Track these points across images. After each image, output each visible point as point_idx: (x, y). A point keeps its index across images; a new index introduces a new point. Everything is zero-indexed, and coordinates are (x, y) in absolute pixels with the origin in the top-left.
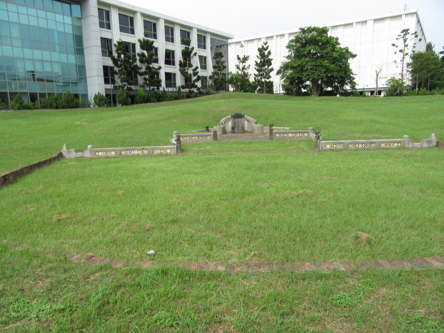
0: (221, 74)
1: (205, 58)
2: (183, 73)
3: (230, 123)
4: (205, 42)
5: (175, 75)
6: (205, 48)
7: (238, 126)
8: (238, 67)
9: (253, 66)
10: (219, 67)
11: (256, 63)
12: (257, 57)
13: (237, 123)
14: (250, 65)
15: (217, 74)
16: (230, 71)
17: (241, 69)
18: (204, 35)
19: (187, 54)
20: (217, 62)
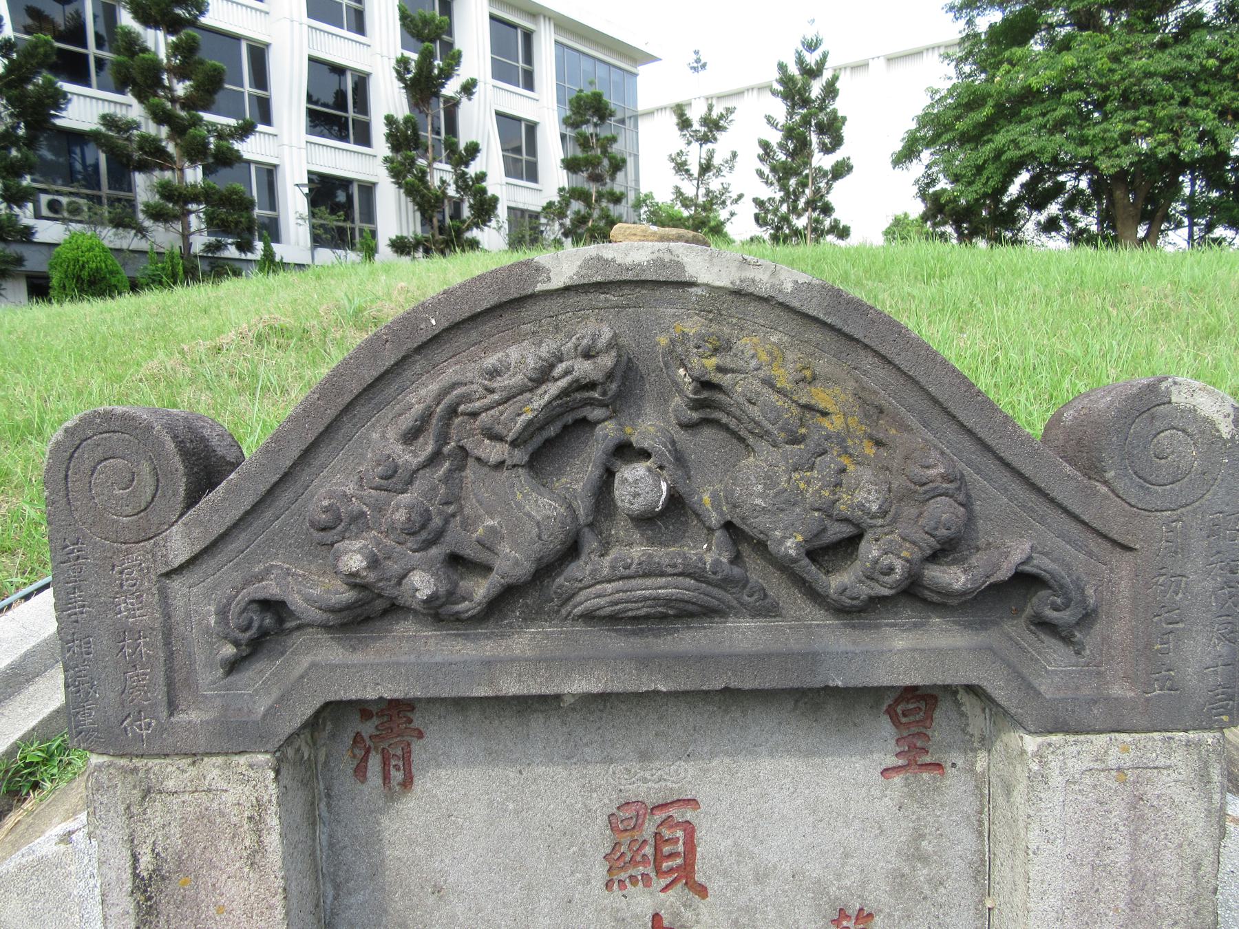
0: (600, 196)
1: (532, 128)
2: (397, 173)
4: (529, 58)
5: (368, 190)
6: (529, 84)
8: (681, 168)
9: (750, 160)
10: (592, 163)
11: (765, 145)
12: (770, 120)
14: (734, 155)
15: (582, 195)
16: (644, 190)
17: (695, 170)
18: (528, 25)
19: (422, 85)
20: (584, 142)
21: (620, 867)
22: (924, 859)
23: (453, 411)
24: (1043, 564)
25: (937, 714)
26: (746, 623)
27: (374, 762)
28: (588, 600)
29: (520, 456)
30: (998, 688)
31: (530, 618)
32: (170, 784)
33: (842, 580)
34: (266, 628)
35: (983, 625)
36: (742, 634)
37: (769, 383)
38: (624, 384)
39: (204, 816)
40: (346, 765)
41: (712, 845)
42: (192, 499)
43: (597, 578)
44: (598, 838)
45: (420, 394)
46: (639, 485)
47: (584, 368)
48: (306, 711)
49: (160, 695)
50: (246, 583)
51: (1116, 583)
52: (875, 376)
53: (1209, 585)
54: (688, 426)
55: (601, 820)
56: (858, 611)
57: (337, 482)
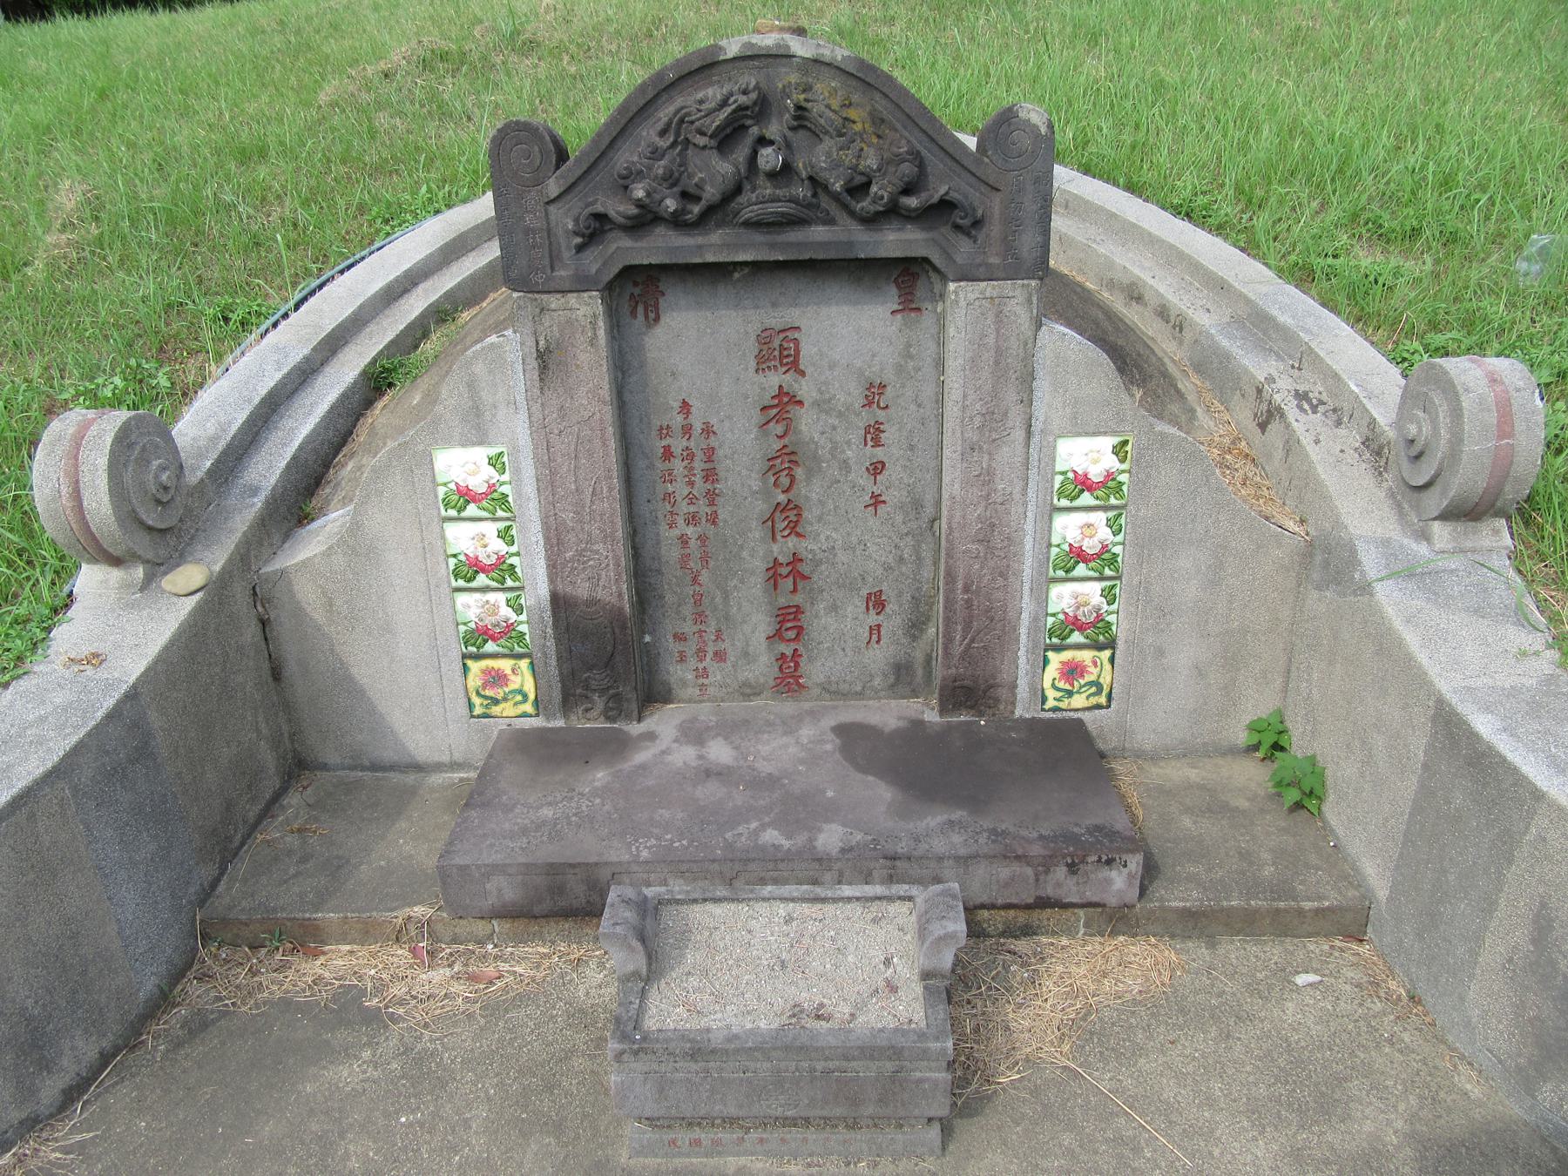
3: (461, 465)
7: (788, 574)
13: (742, 444)
21: (763, 362)
22: (911, 357)
23: (682, 121)
24: (954, 196)
25: (919, 283)
26: (820, 228)
27: (640, 309)
28: (747, 214)
29: (713, 143)
30: (936, 259)
31: (718, 226)
32: (553, 306)
33: (864, 205)
34: (597, 228)
35: (930, 229)
36: (819, 233)
37: (828, 106)
38: (762, 107)
39: (569, 322)
40: (626, 308)
41: (807, 351)
42: (558, 167)
43: (751, 205)
44: (751, 347)
45: (665, 113)
46: (769, 158)
47: (743, 99)
48: (615, 270)
49: (547, 262)
50: (587, 206)
51: (994, 207)
52: (881, 105)
53: (1035, 207)
54: (792, 129)
55: (753, 338)
56: (871, 221)
57: (626, 157)
